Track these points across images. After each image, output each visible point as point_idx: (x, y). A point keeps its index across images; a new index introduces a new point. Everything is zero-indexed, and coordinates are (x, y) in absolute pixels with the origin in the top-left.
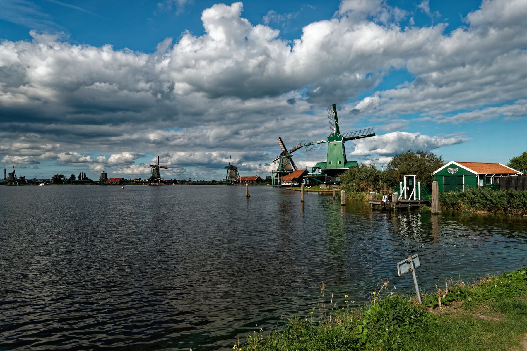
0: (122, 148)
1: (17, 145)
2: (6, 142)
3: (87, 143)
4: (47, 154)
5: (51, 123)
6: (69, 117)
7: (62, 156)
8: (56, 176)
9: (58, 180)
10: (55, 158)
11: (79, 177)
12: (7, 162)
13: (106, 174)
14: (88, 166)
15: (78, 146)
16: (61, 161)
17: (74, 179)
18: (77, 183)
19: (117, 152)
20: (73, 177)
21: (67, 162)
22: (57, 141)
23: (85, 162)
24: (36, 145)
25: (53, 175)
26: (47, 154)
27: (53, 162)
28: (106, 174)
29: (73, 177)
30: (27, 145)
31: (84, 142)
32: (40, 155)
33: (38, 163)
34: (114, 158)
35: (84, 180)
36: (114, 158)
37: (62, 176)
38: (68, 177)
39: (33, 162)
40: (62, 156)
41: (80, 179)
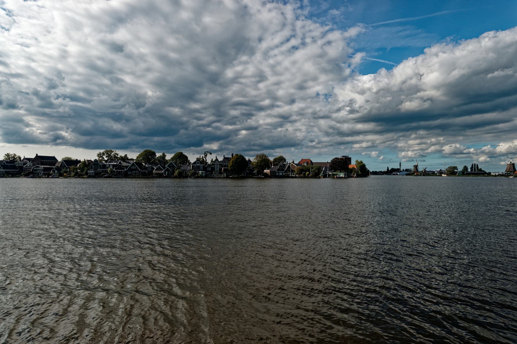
0: (511, 135)
1: (411, 142)
2: (402, 140)
3: (472, 134)
4: (433, 148)
5: (437, 119)
6: (455, 109)
7: (447, 149)
8: (450, 168)
9: (452, 172)
10: (440, 151)
11: (471, 168)
12: (404, 157)
13: (513, 164)
14: (472, 158)
15: (461, 138)
16: (446, 154)
17: (467, 171)
18: (469, 174)
19: (505, 140)
20: (466, 168)
21: (455, 153)
22: (441, 135)
23: (469, 153)
24: (424, 140)
25: (447, 167)
26: (433, 148)
27: (438, 155)
28: (513, 164)
29: (466, 168)
30: (418, 141)
31: (469, 133)
32: (427, 149)
33: (425, 156)
34: (503, 147)
35: (477, 172)
36: (503, 147)
37: (455, 168)
38: (460, 168)
39: (422, 156)
40: (447, 149)
41: (472, 170)
